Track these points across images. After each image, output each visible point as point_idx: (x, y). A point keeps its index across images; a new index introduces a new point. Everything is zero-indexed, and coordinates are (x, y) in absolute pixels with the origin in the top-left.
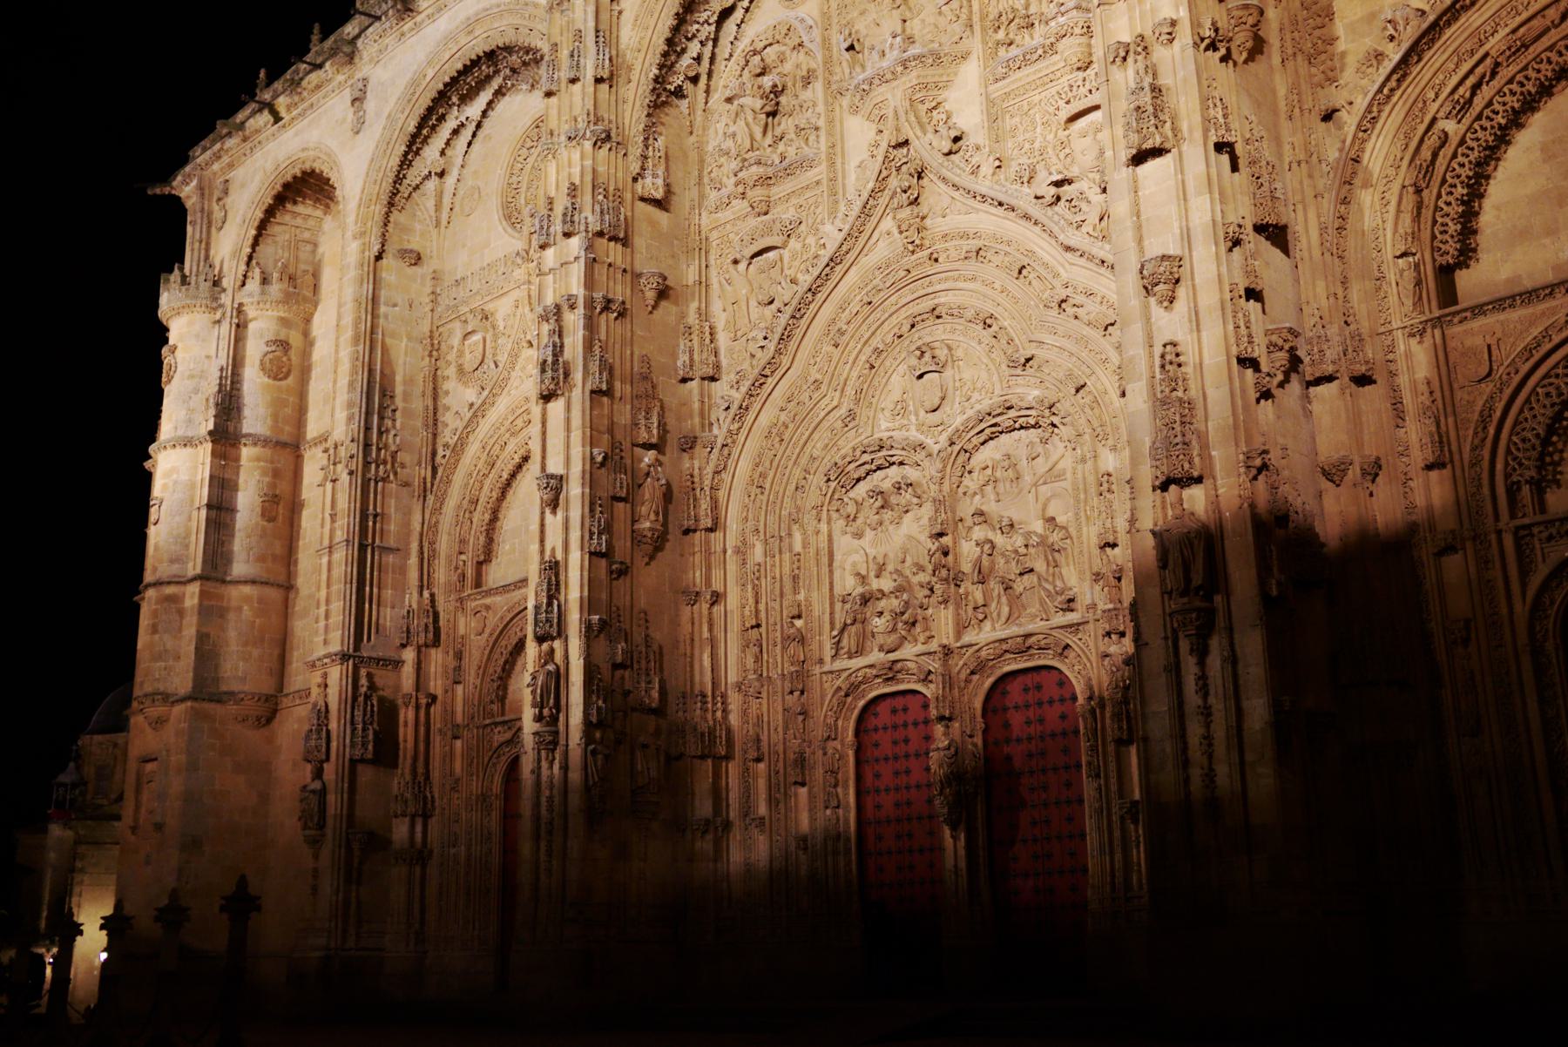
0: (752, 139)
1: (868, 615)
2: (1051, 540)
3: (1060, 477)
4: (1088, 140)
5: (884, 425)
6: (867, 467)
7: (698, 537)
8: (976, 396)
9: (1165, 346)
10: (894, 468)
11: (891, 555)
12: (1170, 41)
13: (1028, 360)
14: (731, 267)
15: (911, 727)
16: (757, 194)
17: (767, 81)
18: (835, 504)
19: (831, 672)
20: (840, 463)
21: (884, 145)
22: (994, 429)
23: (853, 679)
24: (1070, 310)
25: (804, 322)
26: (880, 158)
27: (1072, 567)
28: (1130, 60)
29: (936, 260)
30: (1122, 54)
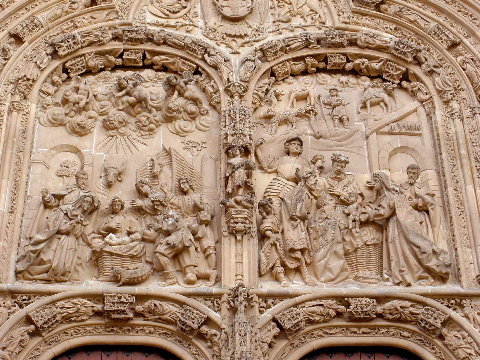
1: (89, 230)
5: (150, 19)
6: (112, 58)
8: (297, 21)
20: (79, 37)
27: (442, 231)
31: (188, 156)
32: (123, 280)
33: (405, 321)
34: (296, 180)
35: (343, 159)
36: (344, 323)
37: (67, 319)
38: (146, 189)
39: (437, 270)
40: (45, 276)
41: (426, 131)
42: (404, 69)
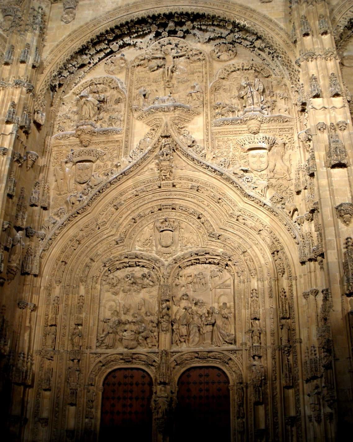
0: (90, 116)
2: (223, 312)
3: (228, 286)
4: (255, 159)
5: (138, 248)
6: (125, 264)
7: (29, 278)
8: (189, 245)
9: (347, 239)
10: (138, 267)
11: (133, 305)
12: (344, 129)
13: (219, 236)
14: (63, 164)
15: (134, 386)
16: (88, 137)
17: (102, 96)
18: (105, 278)
19: (96, 354)
20: (113, 259)
21: (159, 134)
22: (196, 261)
23: (108, 359)
24: (241, 220)
25: (102, 195)
26: (156, 139)
28: (326, 131)
29: (174, 186)
30: (322, 128)
31: (151, 301)
32: (129, 348)
33: (217, 359)
34: (186, 309)
35: (201, 302)
36: (198, 360)
37: (113, 361)
38: (136, 315)
39: (228, 341)
40: (105, 347)
41: (232, 287)
42: (226, 263)
